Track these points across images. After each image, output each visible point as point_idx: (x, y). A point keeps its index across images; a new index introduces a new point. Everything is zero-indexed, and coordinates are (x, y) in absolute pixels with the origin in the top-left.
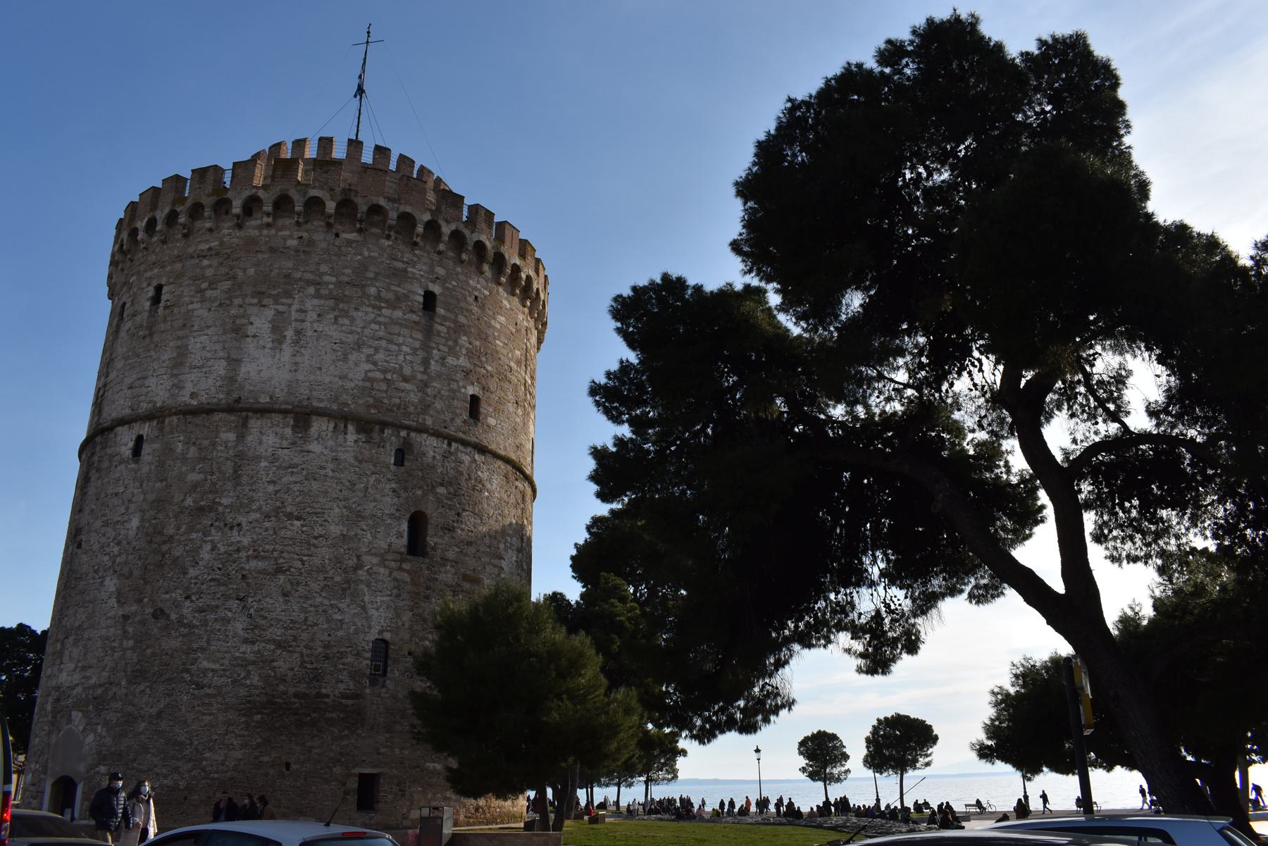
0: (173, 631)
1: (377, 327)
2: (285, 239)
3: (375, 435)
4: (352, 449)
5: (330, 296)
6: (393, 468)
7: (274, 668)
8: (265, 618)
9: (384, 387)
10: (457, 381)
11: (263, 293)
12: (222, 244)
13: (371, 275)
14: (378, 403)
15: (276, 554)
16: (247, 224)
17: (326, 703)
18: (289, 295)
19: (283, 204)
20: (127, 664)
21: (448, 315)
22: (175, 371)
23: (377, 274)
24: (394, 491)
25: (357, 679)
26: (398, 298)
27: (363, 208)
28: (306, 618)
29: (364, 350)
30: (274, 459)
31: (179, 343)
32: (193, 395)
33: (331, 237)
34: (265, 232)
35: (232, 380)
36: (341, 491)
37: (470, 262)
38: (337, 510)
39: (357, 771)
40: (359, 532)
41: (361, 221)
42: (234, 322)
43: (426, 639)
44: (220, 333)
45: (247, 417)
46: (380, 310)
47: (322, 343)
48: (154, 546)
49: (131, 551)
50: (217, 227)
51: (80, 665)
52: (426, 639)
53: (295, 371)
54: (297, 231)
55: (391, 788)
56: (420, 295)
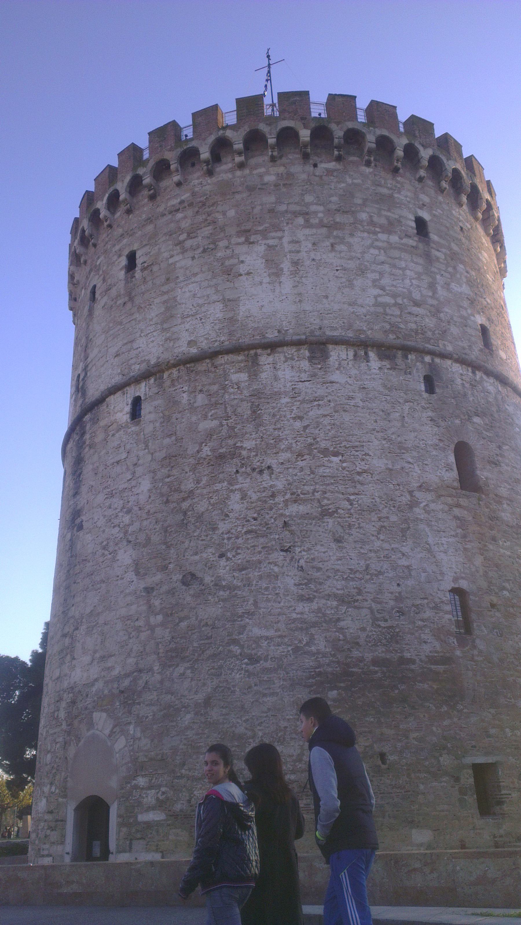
0: (210, 597)
1: (376, 252)
2: (261, 176)
3: (399, 361)
4: (378, 376)
5: (321, 225)
6: (425, 395)
7: (342, 629)
8: (319, 569)
10: (466, 309)
11: (249, 231)
12: (194, 194)
14: (394, 328)
15: (317, 495)
16: (218, 169)
17: (413, 671)
18: (277, 228)
20: (157, 644)
21: (442, 242)
22: (165, 326)
23: (365, 200)
25: (442, 637)
28: (367, 567)
29: (368, 275)
30: (295, 394)
31: (166, 297)
32: (190, 343)
33: (309, 168)
34: (238, 173)
35: (232, 320)
36: (376, 421)
38: (376, 442)
39: (469, 760)
40: (406, 465)
41: (338, 147)
42: (222, 264)
43: (504, 588)
44: (209, 277)
45: (256, 355)
46: (377, 235)
48: (172, 506)
49: (145, 516)
50: (186, 180)
51: (97, 655)
52: (504, 588)
53: (300, 301)
54: (272, 166)
55: (513, 783)
56: (411, 220)
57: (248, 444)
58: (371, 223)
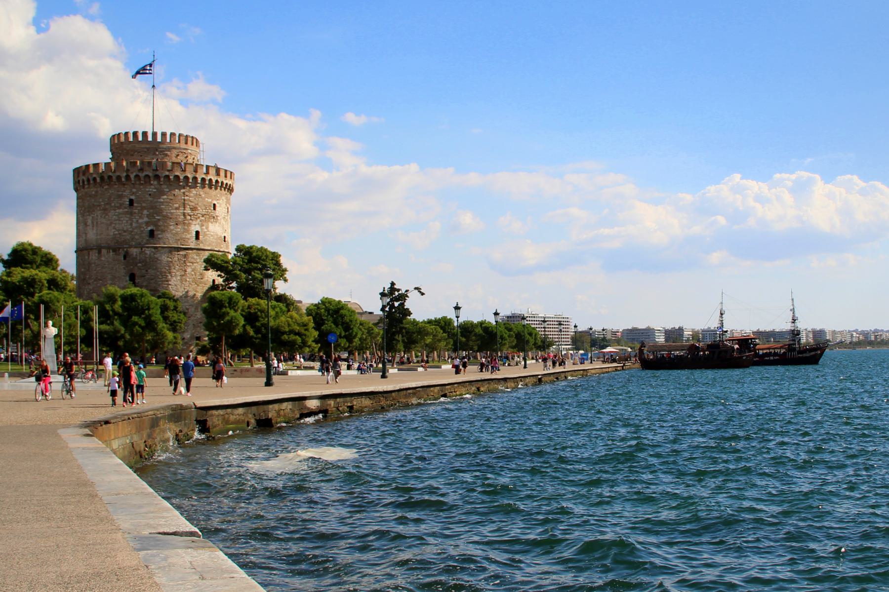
5: (103, 210)
19: (89, 180)
24: (124, 268)
27: (106, 178)
37: (146, 182)
45: (89, 252)
58: (115, 206)
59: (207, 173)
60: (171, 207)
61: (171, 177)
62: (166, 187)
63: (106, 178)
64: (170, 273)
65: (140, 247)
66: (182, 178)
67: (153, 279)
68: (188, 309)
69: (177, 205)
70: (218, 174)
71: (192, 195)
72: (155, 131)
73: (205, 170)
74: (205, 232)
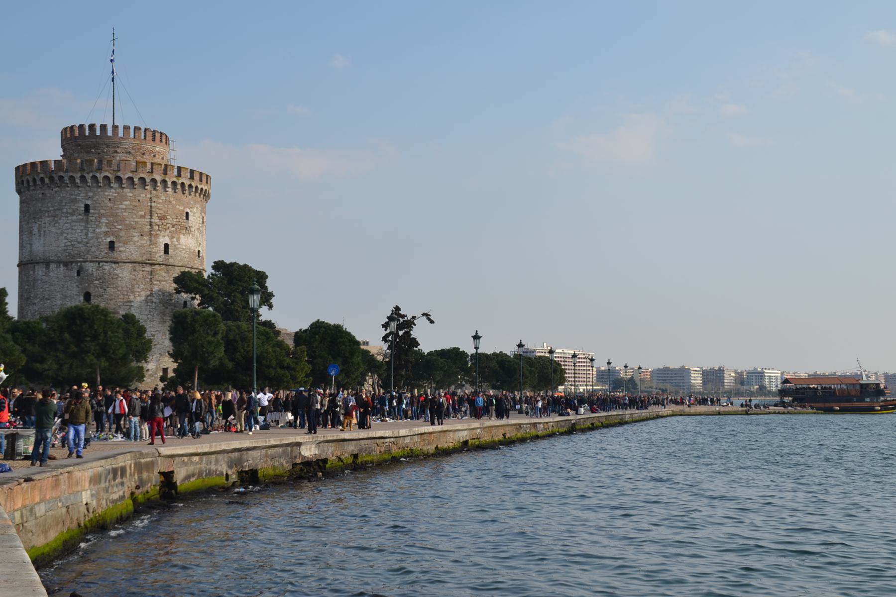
3: (69, 266)
5: (52, 216)
6: (76, 277)
9: (71, 248)
10: (101, 238)
13: (64, 204)
23: (66, 203)
24: (77, 286)
26: (74, 211)
27: (56, 178)
33: (51, 191)
37: (105, 185)
47: (51, 234)
57: (32, 295)
58: (67, 213)
59: (179, 175)
60: (135, 214)
61: (135, 180)
62: (129, 190)
63: (56, 178)
64: (133, 292)
65: (96, 262)
66: (148, 180)
67: (112, 300)
68: (153, 336)
69: (142, 213)
70: (192, 177)
71: (160, 201)
72: (115, 124)
73: (176, 173)
74: (175, 246)
